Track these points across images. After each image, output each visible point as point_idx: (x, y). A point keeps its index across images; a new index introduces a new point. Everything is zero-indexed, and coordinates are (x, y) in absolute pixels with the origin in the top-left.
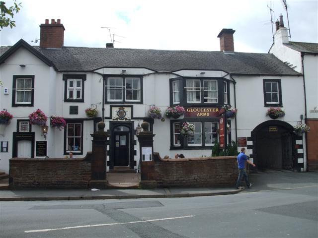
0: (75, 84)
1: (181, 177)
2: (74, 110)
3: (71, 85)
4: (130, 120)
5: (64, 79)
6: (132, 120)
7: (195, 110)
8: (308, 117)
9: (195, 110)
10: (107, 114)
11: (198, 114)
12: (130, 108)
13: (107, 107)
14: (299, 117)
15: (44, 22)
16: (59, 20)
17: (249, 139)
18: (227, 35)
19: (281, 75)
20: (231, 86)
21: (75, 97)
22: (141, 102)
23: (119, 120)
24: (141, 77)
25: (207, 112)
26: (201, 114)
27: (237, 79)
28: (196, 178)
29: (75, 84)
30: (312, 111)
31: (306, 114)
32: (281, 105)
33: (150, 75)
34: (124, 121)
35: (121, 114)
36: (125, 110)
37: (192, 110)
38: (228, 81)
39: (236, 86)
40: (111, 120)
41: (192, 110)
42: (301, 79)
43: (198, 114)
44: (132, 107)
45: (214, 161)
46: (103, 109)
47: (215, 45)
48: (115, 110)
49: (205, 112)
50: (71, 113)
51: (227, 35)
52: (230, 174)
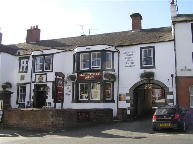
0: (25, 62)
1: (17, 122)
2: (22, 78)
3: (23, 63)
4: (45, 83)
5: (19, 60)
6: (46, 83)
7: (84, 75)
8: (178, 75)
9: (84, 75)
10: (33, 80)
11: (86, 78)
12: (45, 75)
13: (34, 75)
14: (171, 76)
15: (30, 28)
16: (37, 26)
17: (127, 95)
18: (136, 18)
19: (155, 43)
20: (116, 55)
21: (24, 70)
22: (52, 71)
23: (39, 83)
24: (52, 54)
25: (92, 76)
26: (88, 77)
27: (119, 49)
28: (25, 123)
29: (25, 62)
30: (182, 70)
31: (176, 73)
32: (154, 67)
33: (59, 53)
34: (42, 83)
35: (41, 79)
36: (43, 77)
37: (82, 75)
38: (113, 52)
39: (120, 55)
40: (35, 83)
41: (82, 75)
42: (173, 42)
43: (86, 78)
44: (46, 74)
45: (35, 112)
46: (31, 77)
47: (127, 26)
48: (38, 77)
49: (91, 76)
50: (21, 80)
51: (136, 18)
52: (45, 122)
